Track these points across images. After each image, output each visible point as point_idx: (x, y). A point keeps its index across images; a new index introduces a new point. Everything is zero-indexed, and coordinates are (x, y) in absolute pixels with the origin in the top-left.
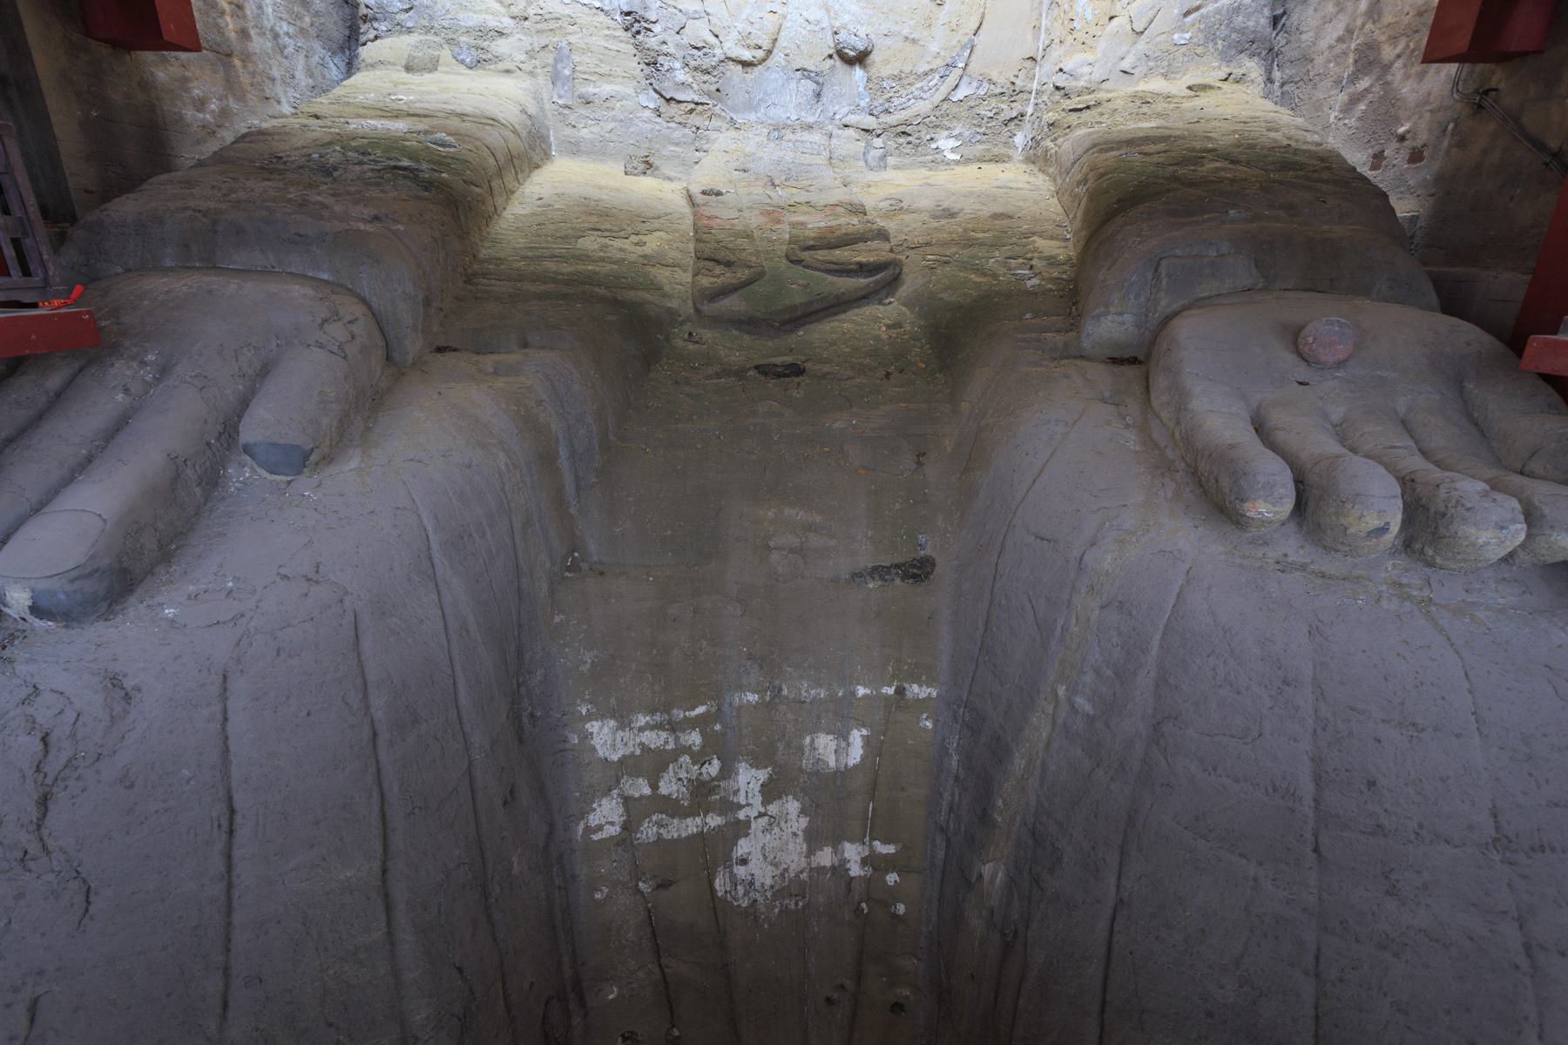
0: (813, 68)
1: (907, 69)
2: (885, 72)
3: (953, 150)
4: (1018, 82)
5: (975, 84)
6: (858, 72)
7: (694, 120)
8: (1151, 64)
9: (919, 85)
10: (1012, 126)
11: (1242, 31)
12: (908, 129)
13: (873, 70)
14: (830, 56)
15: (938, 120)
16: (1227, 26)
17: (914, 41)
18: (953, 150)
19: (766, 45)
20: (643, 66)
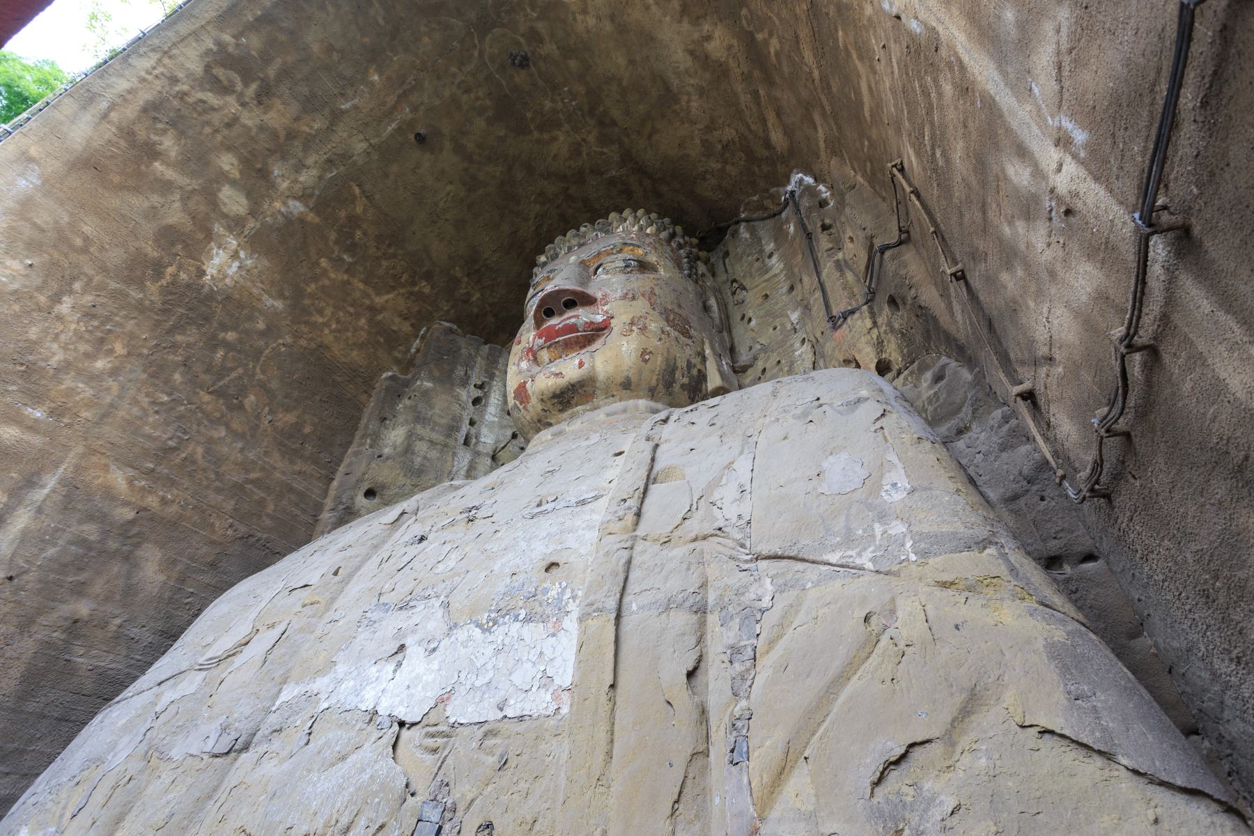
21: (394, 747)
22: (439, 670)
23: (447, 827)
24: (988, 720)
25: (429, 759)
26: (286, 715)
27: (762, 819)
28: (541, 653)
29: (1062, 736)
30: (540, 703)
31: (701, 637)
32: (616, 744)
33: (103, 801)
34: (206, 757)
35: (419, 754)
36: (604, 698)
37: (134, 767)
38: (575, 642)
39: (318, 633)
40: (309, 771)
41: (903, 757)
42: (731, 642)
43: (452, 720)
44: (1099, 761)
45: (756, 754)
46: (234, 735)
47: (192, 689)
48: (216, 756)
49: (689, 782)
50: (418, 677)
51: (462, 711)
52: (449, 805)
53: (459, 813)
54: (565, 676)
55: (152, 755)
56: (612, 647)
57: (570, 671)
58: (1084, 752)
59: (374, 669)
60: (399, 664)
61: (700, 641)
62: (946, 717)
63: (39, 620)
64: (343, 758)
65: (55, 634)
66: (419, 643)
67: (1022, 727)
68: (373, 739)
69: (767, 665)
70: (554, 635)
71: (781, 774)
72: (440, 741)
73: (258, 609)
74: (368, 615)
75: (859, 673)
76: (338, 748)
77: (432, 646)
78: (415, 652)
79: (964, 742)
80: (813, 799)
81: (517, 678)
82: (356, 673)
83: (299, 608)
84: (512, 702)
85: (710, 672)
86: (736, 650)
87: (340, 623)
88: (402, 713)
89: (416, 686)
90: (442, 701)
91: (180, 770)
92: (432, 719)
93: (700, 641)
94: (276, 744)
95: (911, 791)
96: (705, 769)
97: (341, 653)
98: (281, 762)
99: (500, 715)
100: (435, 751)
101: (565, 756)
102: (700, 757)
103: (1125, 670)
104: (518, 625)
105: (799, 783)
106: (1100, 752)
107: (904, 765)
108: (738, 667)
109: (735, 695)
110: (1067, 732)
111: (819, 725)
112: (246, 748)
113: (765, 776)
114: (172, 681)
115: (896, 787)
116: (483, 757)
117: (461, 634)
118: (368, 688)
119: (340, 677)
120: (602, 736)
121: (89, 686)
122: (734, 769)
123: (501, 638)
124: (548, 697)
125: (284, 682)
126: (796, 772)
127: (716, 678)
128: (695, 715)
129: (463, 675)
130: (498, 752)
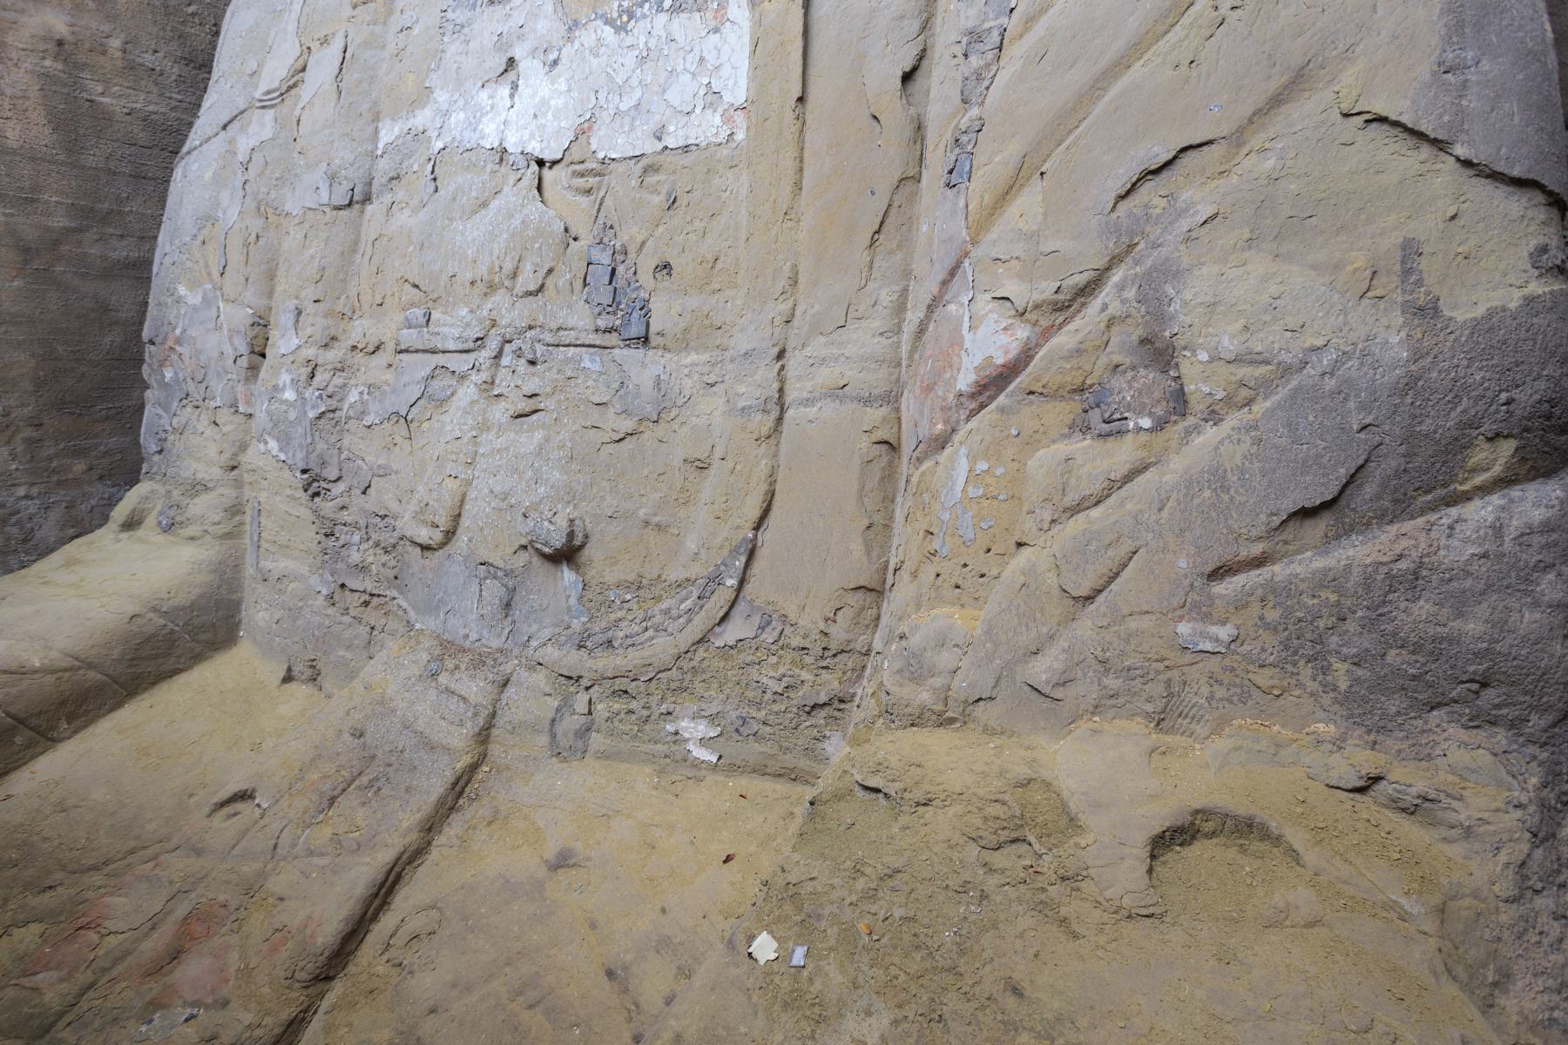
0: (501, 564)
1: (651, 571)
2: (610, 578)
3: (703, 742)
4: (834, 630)
5: (756, 620)
6: (568, 575)
7: (371, 616)
8: (1112, 683)
9: (665, 605)
10: (820, 717)
11: (1435, 648)
12: (632, 687)
13: (591, 573)
14: (525, 547)
15: (676, 679)
16: (1369, 625)
17: (658, 526)
18: (703, 742)
19: (443, 521)
20: (320, 537)
21: (539, 188)
22: (569, 91)
23: (621, 269)
24: (1306, 112)
25: (584, 201)
26: (398, 159)
27: (974, 242)
28: (702, 59)
29: (1396, 124)
30: (708, 127)
31: (927, 21)
32: (806, 173)
33: (243, 259)
34: (327, 210)
35: (570, 196)
36: (789, 115)
37: (256, 225)
38: (747, 40)
39: (391, 48)
40: (451, 219)
41: (1168, 164)
42: (970, 24)
43: (601, 155)
44: (1426, 151)
45: (981, 172)
46: (346, 186)
47: (267, 134)
48: (339, 208)
49: (893, 211)
50: (544, 102)
51: (611, 142)
52: (618, 247)
53: (632, 255)
54: (737, 89)
55: (266, 210)
56: (799, 43)
57: (743, 83)
58: (1411, 141)
59: (484, 95)
60: (515, 87)
61: (925, 26)
62: (1247, 109)
63: (9, 39)
64: (484, 205)
65: (47, 63)
66: (533, 53)
67: (1346, 115)
68: (512, 182)
69: (1016, 53)
70: (716, 30)
71: (1007, 193)
72: (592, 181)
73: (294, 16)
74: (449, 15)
75: (1146, 57)
76: (474, 194)
77: (552, 57)
78: (529, 67)
79: (1256, 142)
80: (1040, 218)
81: (673, 96)
82: (461, 102)
83: (348, 11)
84: (672, 129)
85: (935, 73)
86: (975, 36)
87: (416, 31)
88: (536, 148)
89: (545, 115)
90: (582, 132)
91: (306, 225)
92: (576, 154)
93: (925, 26)
94: (400, 194)
95: (1163, 203)
96: (914, 197)
97: (433, 76)
98: (415, 211)
99: (660, 146)
100: (589, 192)
101: (744, 191)
102: (910, 182)
103: (1548, 27)
104: (664, 17)
105: (1029, 203)
106: (1435, 142)
107: (1165, 174)
108: (975, 61)
109: (965, 101)
110: (1404, 119)
111: (1070, 132)
112: (367, 199)
113: (987, 196)
114: (236, 124)
115: (1146, 199)
116: (647, 196)
117: (586, 37)
118: (485, 120)
119: (444, 107)
120: (789, 164)
121: (143, 137)
122: (949, 192)
123: (642, 39)
124: (718, 120)
125: (376, 118)
126: (1026, 190)
127: (941, 81)
128: (908, 131)
129: (602, 96)
130: (665, 189)
